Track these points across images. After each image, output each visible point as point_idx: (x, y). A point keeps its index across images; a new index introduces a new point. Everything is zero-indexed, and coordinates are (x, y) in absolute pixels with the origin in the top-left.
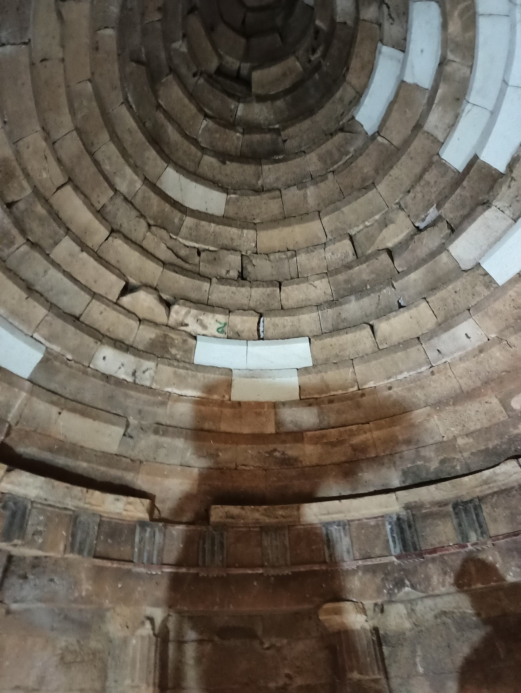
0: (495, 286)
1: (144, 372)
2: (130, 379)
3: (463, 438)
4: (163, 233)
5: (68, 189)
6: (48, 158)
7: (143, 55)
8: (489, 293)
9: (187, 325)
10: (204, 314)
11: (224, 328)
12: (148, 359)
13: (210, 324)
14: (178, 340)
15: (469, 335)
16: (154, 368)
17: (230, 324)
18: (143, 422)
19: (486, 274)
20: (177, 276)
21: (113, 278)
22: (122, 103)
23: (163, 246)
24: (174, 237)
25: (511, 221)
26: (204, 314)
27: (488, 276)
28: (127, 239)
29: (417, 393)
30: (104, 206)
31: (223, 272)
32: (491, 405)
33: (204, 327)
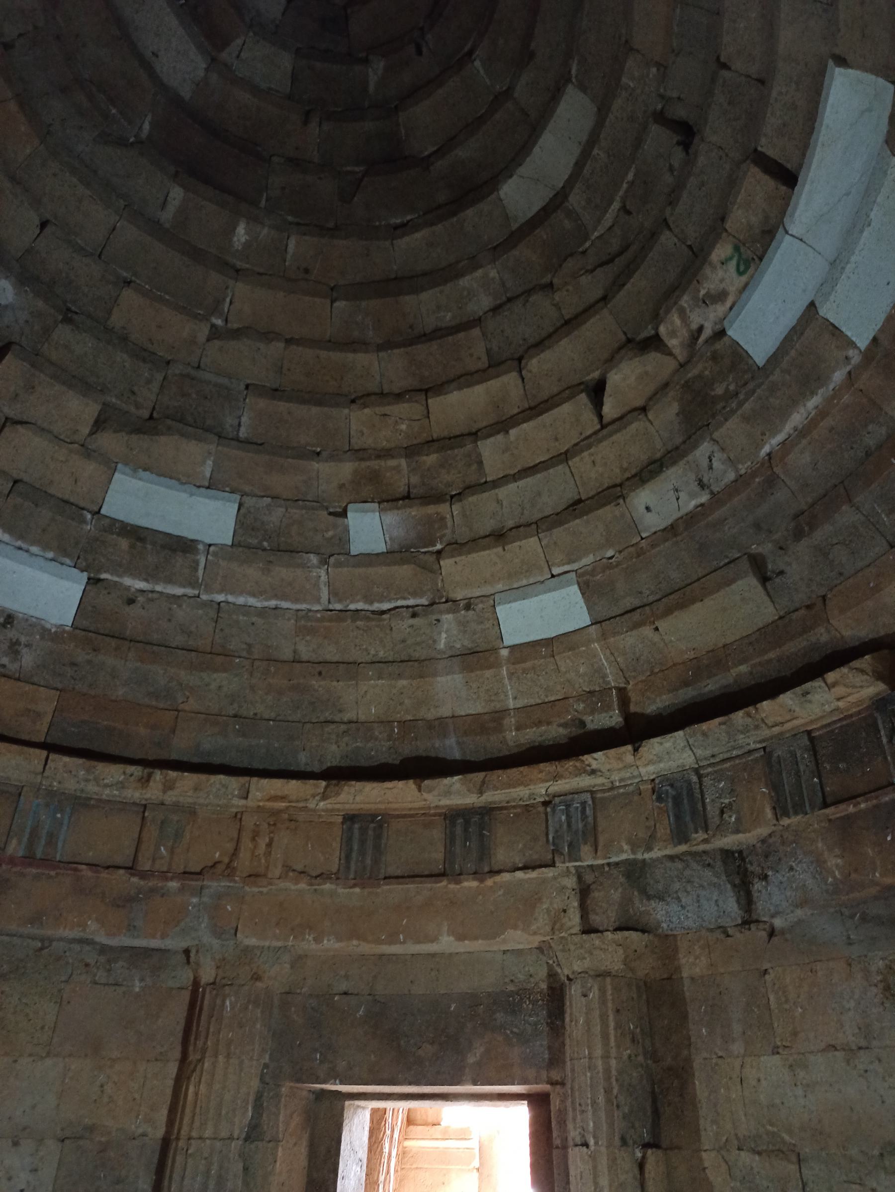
1: (711, 467)
2: (704, 498)
4: (570, 264)
5: (434, 402)
6: (388, 413)
7: (357, 169)
9: (701, 329)
10: (698, 282)
11: (744, 257)
12: (695, 446)
13: (722, 281)
14: (706, 368)
16: (716, 448)
17: (741, 237)
18: (776, 536)
20: (628, 286)
21: (566, 408)
22: (392, 244)
23: (584, 280)
24: (587, 244)
26: (698, 282)
28: (540, 345)
30: (489, 352)
31: (669, 179)
33: (720, 297)
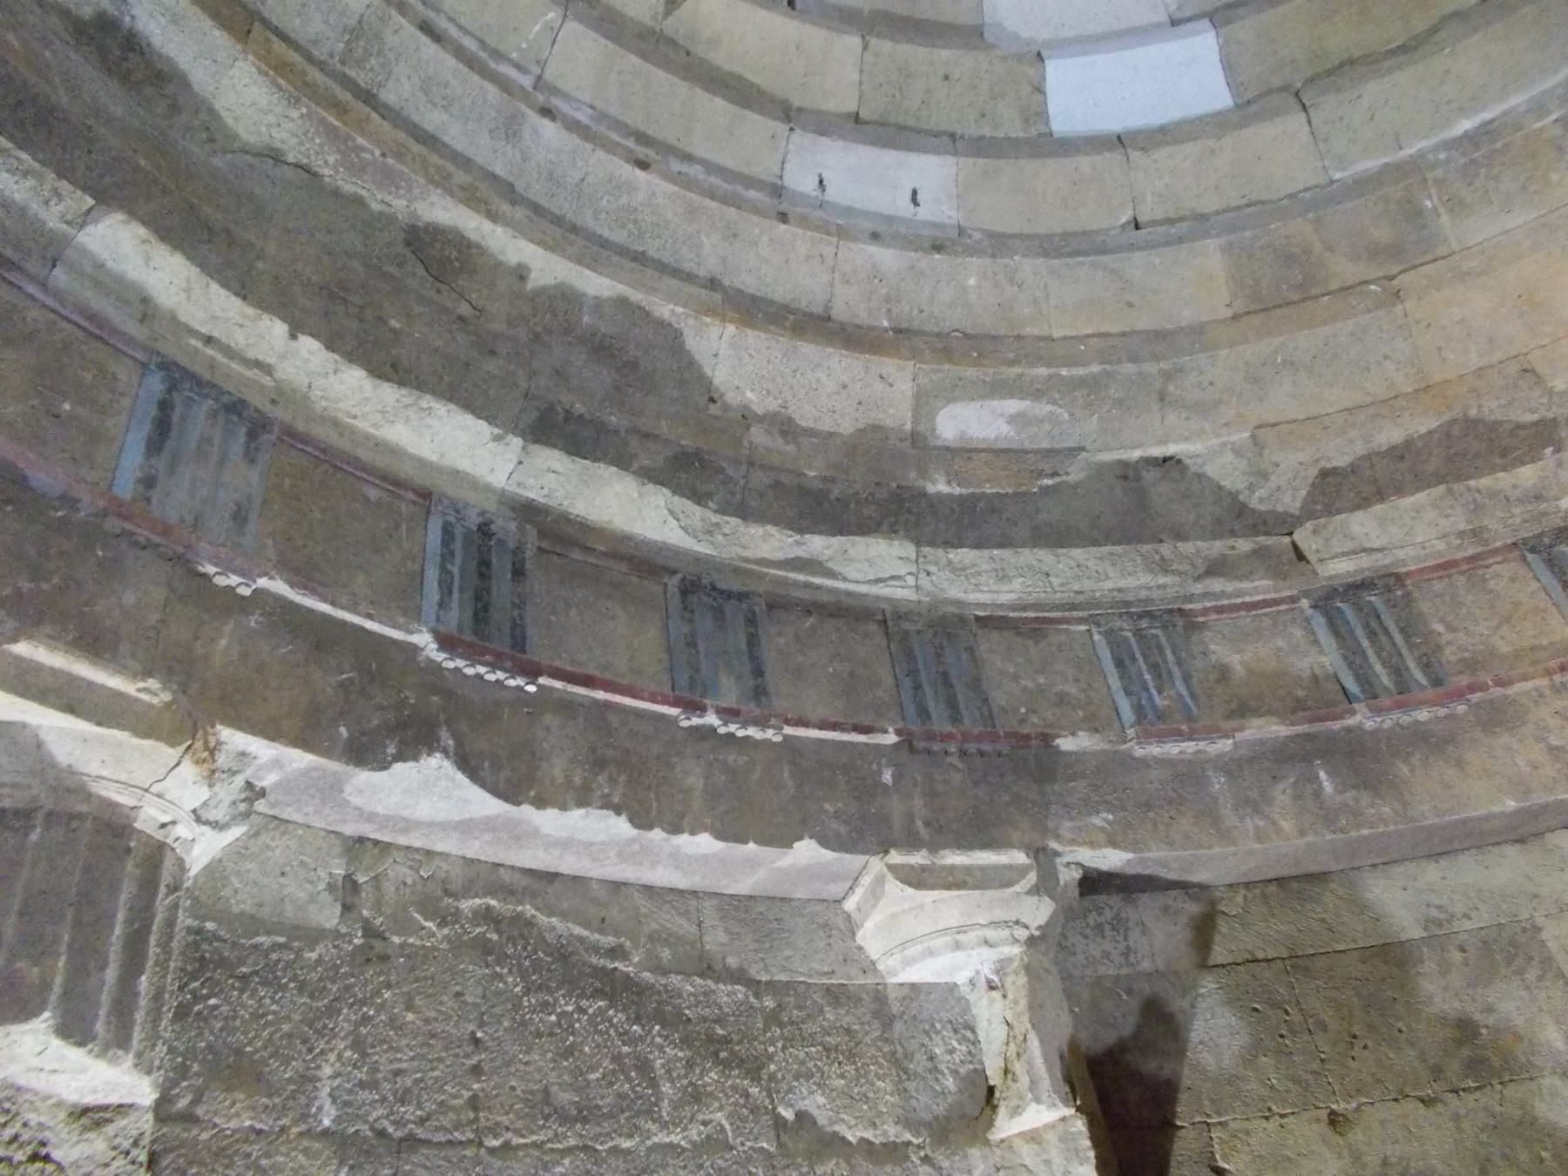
0: (1043, 129)
3: (768, 432)
8: (1021, 134)
15: (920, 197)
19: (1040, 90)
25: (1163, 18)
27: (1041, 97)
29: (706, 241)
32: (888, 389)
